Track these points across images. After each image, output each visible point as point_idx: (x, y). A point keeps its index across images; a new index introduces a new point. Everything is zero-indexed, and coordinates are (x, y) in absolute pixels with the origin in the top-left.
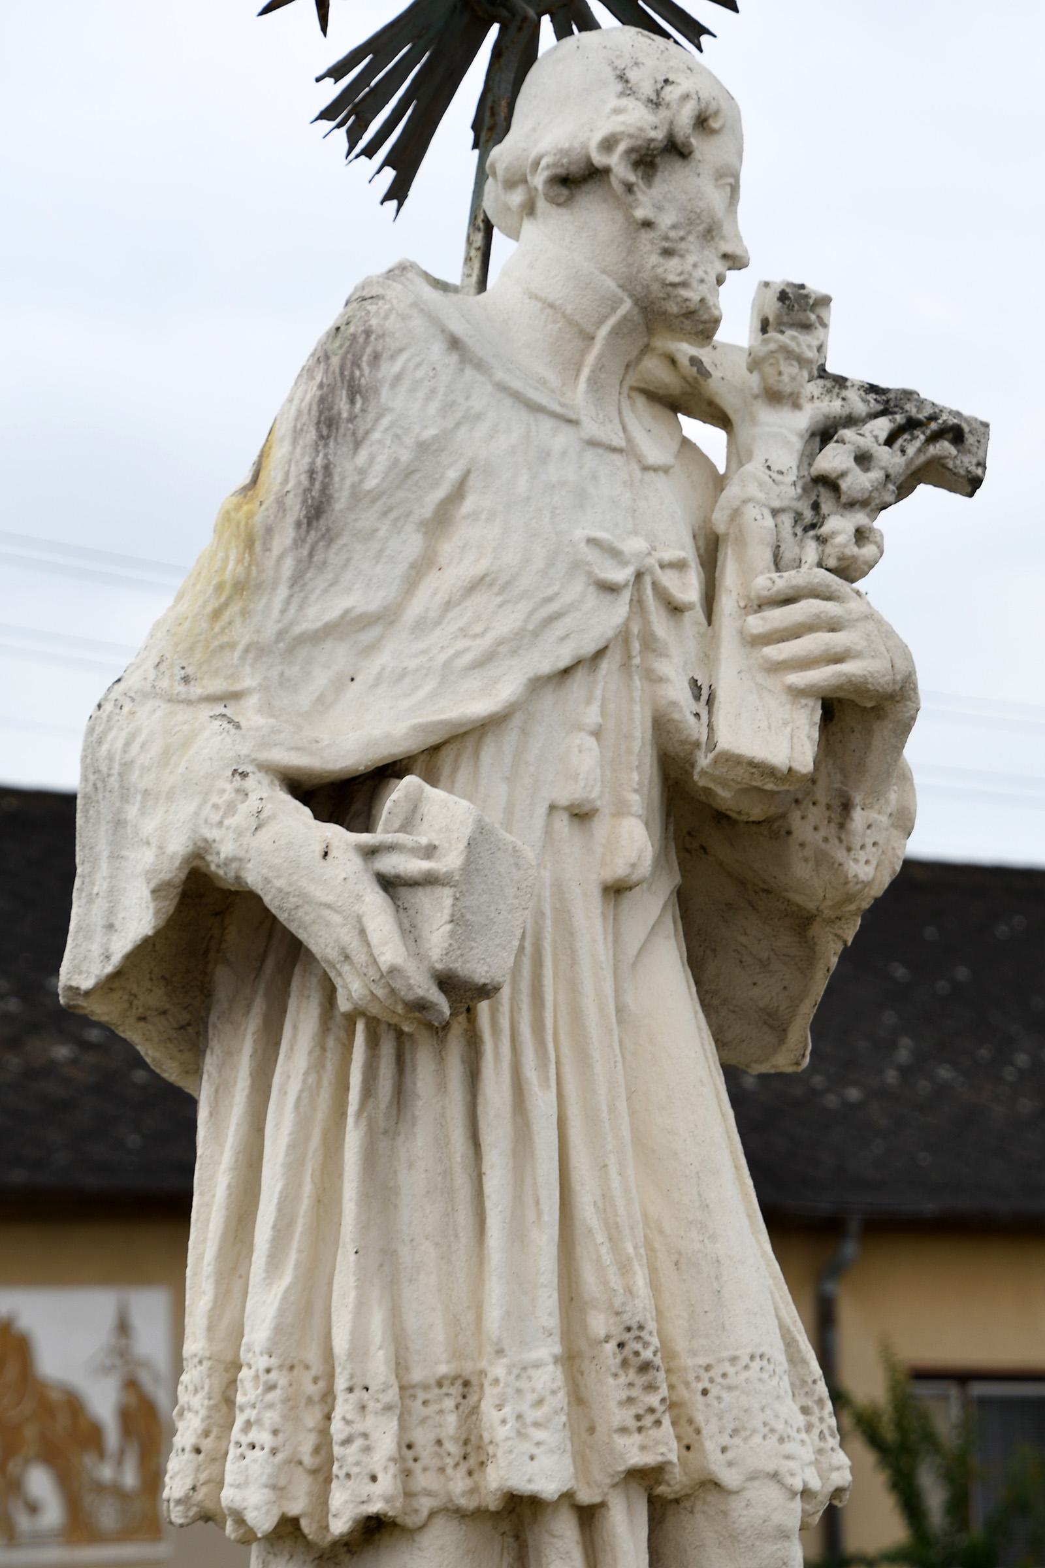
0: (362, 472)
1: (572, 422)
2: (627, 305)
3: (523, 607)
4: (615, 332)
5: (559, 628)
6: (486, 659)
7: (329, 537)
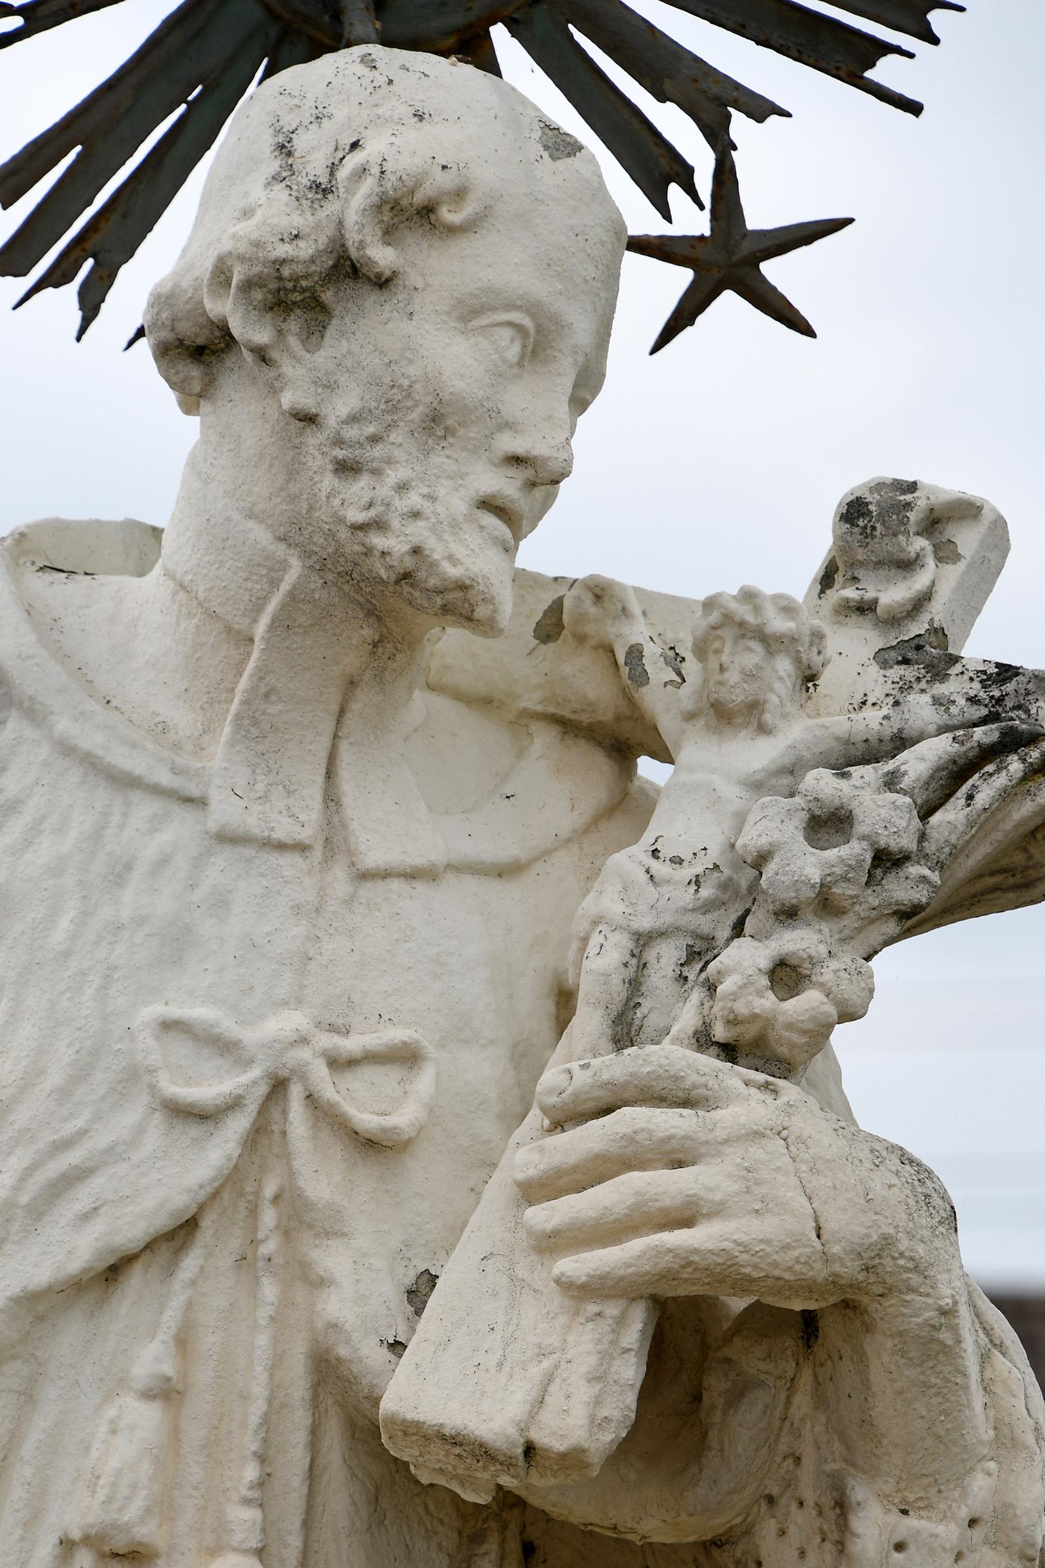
1: (197, 802)
2: (295, 570)
4: (282, 624)
5: (82, 1198)
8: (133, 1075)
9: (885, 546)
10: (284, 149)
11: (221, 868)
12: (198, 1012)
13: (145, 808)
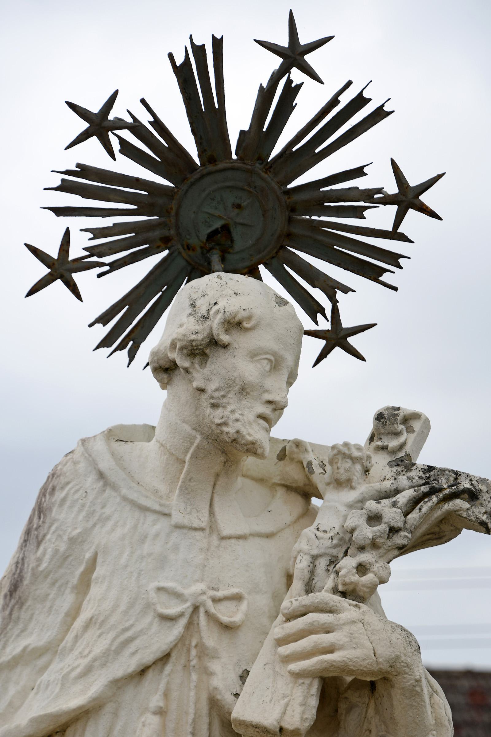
0: (39, 560)
1: (168, 515)
3: (111, 635)
4: (195, 456)
5: (132, 647)
6: (88, 671)
7: (21, 603)
8: (148, 606)
9: (390, 428)
10: (193, 305)
11: (176, 536)
12: (169, 584)
13: (151, 517)
